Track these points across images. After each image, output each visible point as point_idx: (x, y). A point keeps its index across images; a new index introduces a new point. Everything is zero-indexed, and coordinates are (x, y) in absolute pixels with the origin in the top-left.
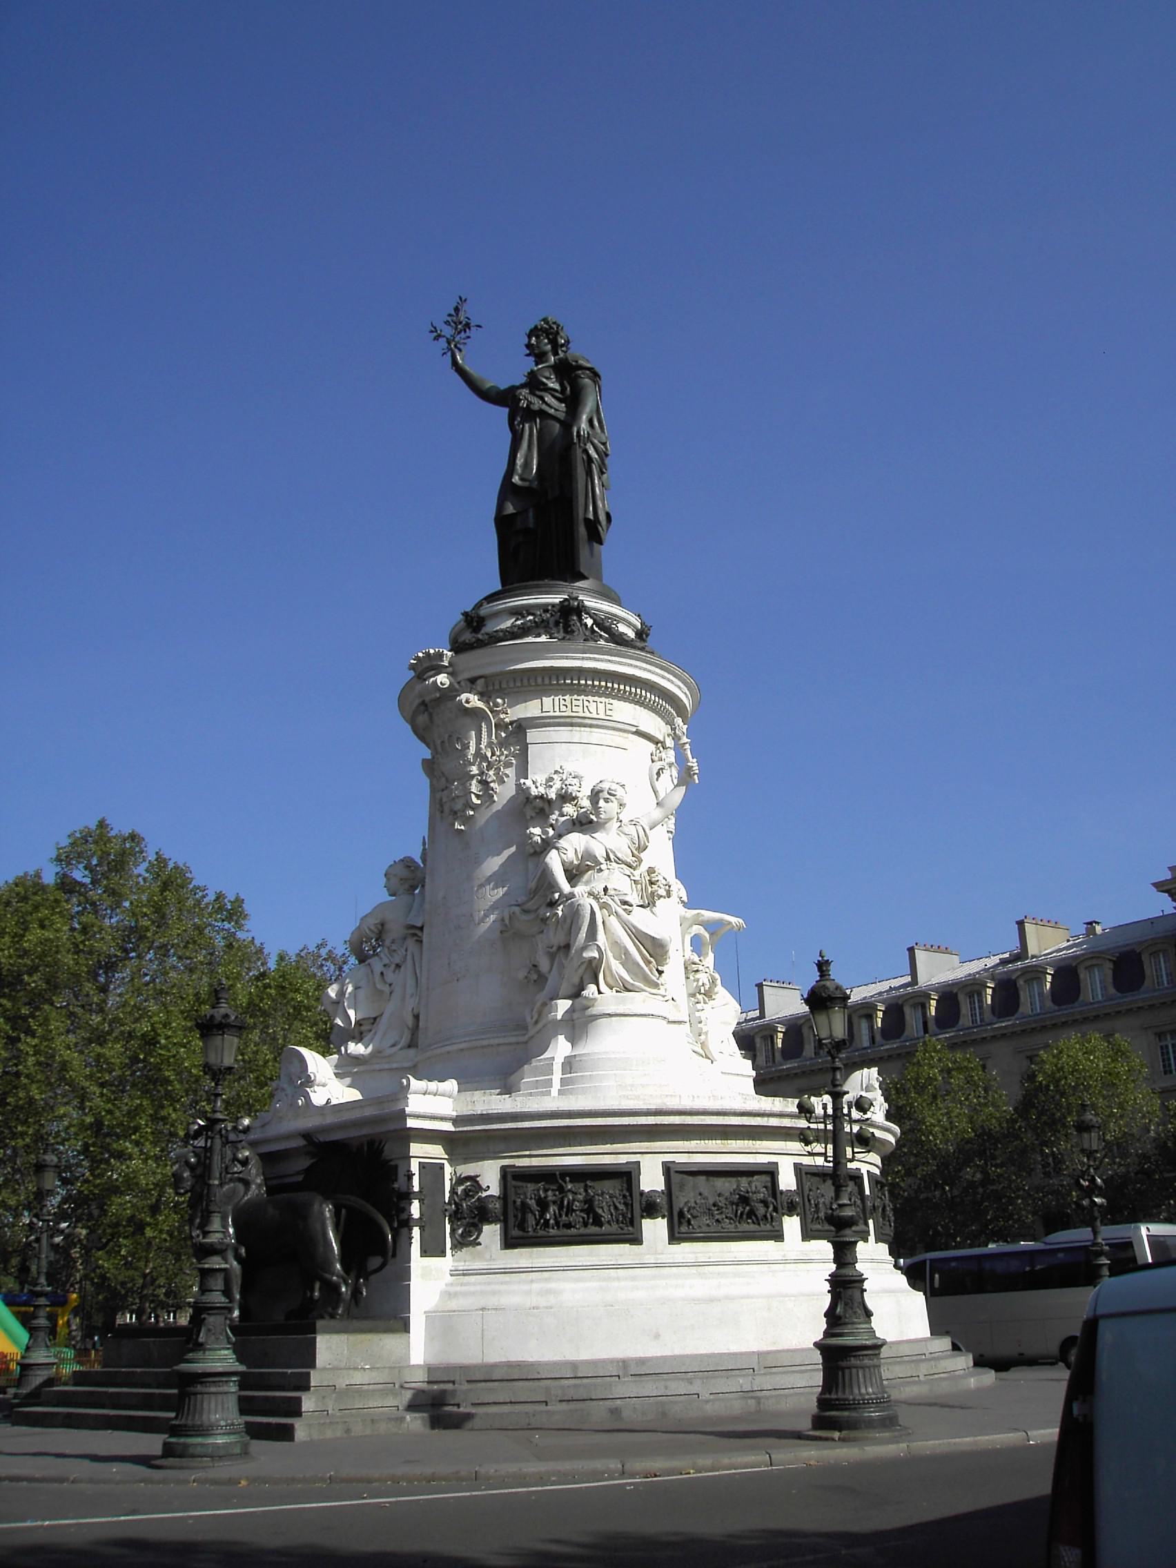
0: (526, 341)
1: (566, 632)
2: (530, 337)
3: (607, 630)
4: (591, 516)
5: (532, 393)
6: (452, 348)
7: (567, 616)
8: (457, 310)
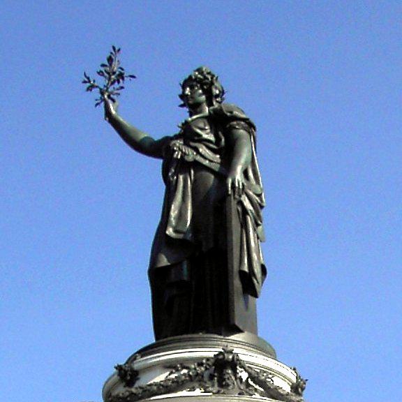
0: (180, 91)
1: (221, 385)
2: (184, 87)
3: (262, 384)
4: (246, 269)
5: (186, 144)
6: (105, 99)
7: (222, 368)
8: (110, 60)
